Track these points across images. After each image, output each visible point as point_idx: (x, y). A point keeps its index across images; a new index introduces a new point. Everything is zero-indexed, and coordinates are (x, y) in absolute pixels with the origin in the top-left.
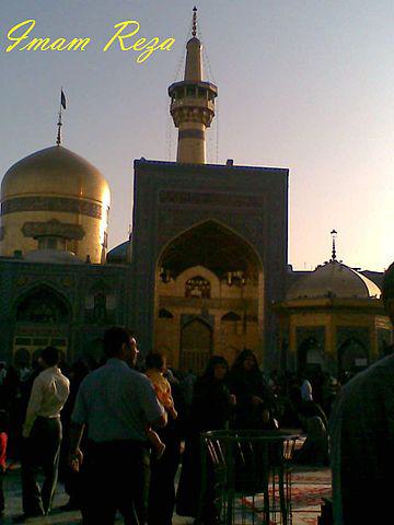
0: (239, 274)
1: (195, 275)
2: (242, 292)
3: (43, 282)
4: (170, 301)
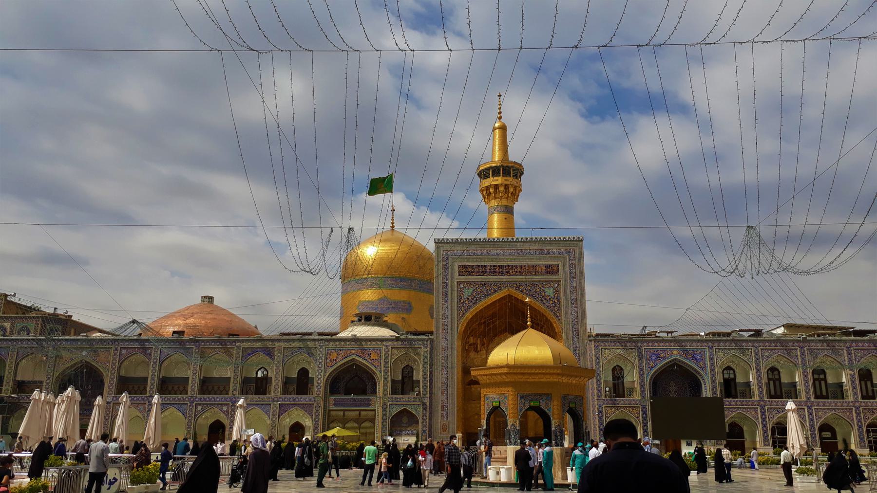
3: (353, 357)
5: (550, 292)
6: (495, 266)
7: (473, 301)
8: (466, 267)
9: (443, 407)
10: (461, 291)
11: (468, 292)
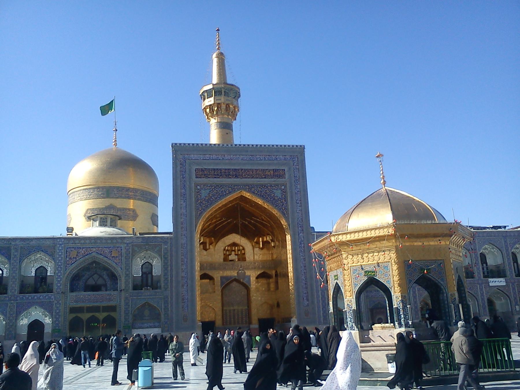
0: (269, 238)
1: (231, 242)
2: (272, 254)
3: (94, 254)
4: (213, 266)
5: (278, 193)
6: (228, 169)
7: (210, 202)
8: (202, 170)
9: (183, 299)
10: (198, 192)
11: (204, 193)
